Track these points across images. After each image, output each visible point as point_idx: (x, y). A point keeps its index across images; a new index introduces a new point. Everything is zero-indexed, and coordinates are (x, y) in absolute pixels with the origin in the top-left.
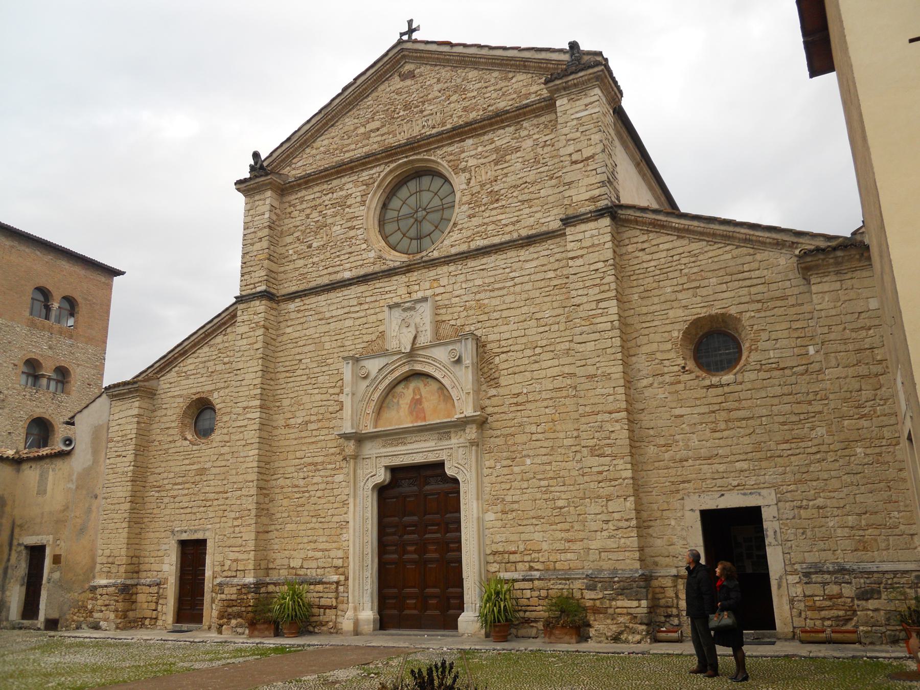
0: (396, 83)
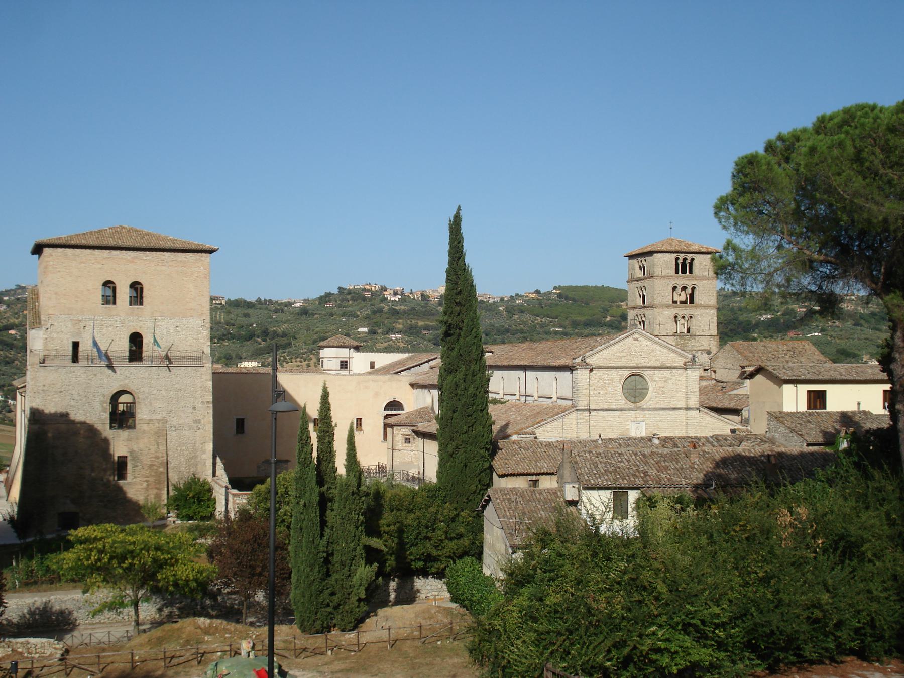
0: (631, 339)
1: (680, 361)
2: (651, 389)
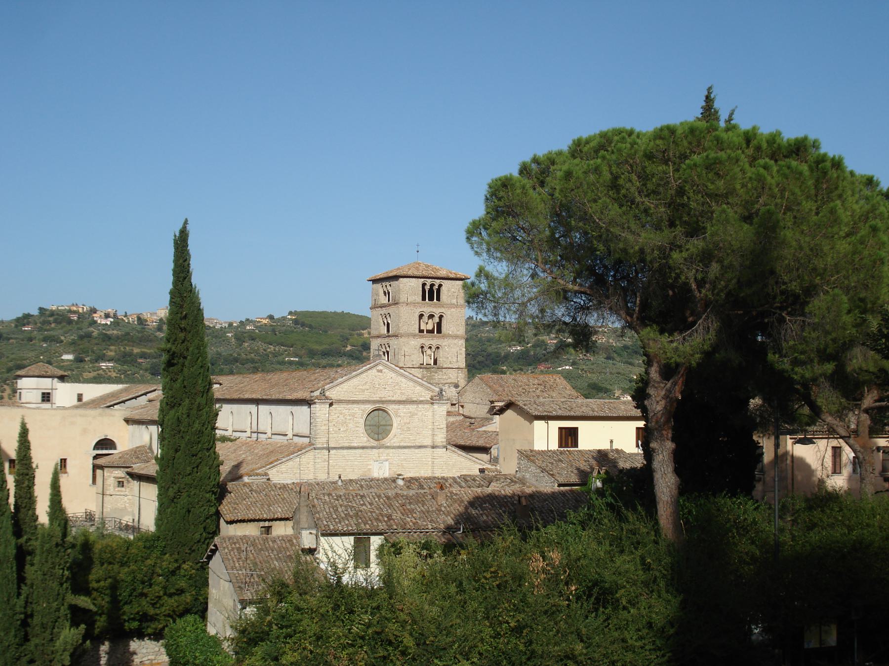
0: (374, 370)
1: (427, 395)
2: (395, 425)
